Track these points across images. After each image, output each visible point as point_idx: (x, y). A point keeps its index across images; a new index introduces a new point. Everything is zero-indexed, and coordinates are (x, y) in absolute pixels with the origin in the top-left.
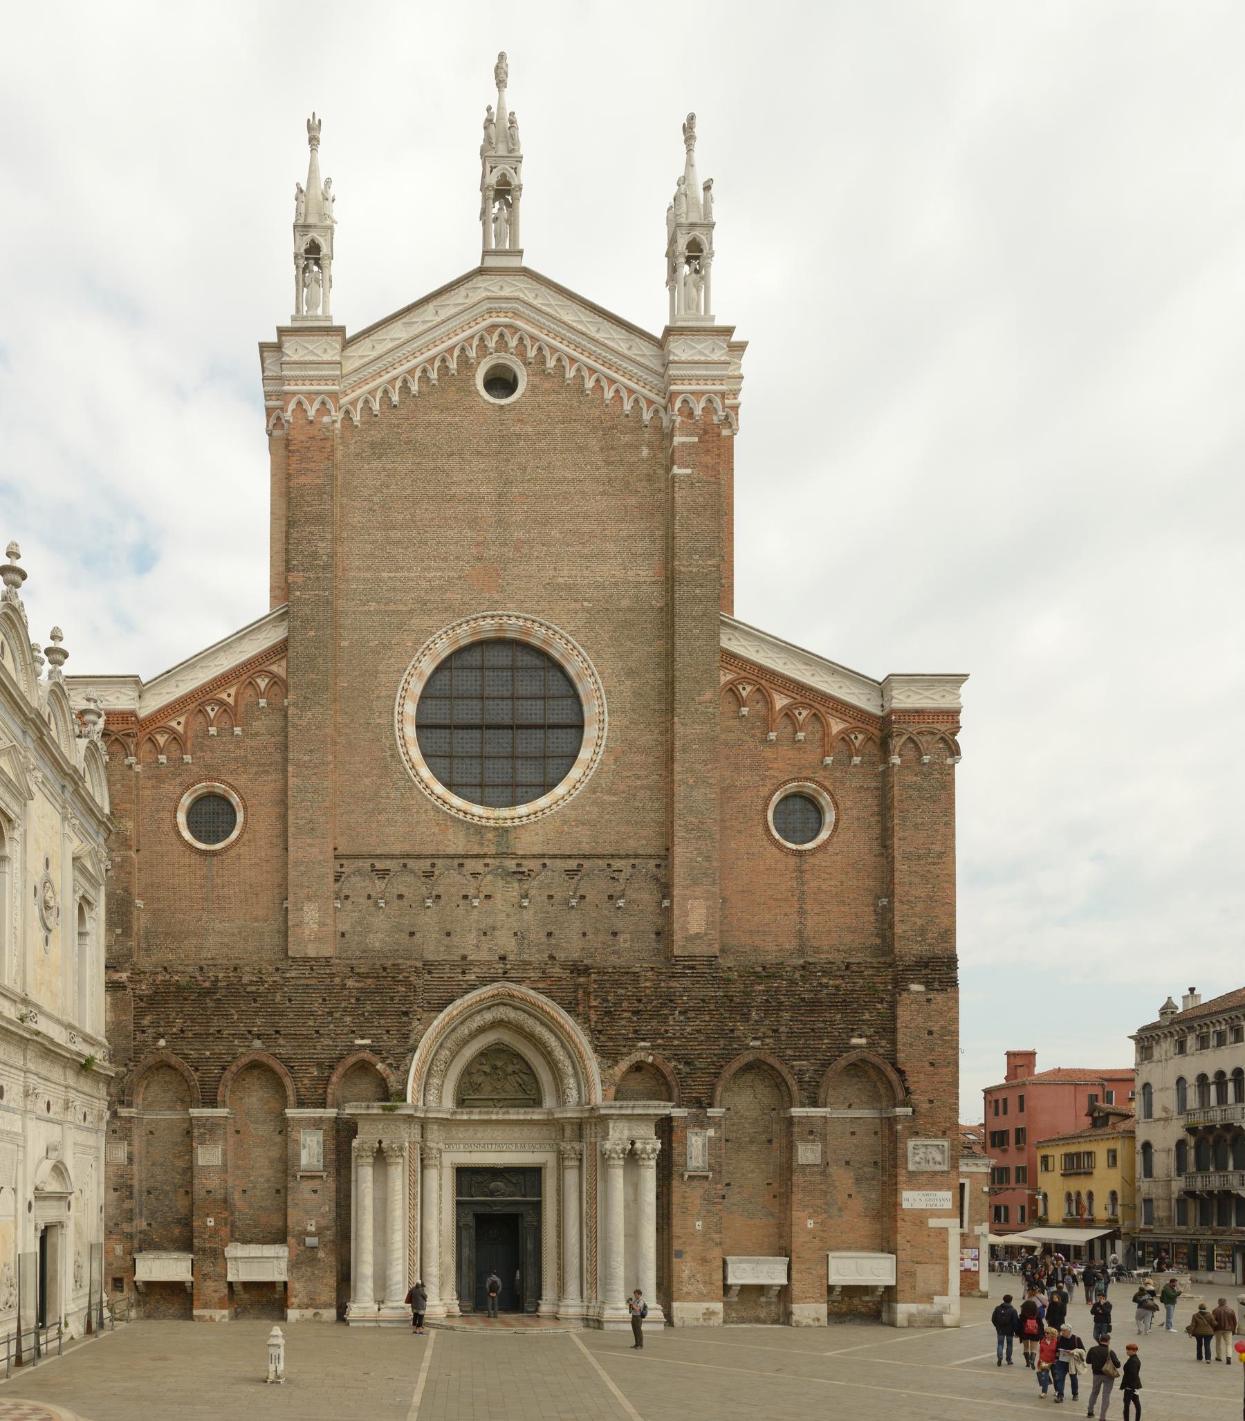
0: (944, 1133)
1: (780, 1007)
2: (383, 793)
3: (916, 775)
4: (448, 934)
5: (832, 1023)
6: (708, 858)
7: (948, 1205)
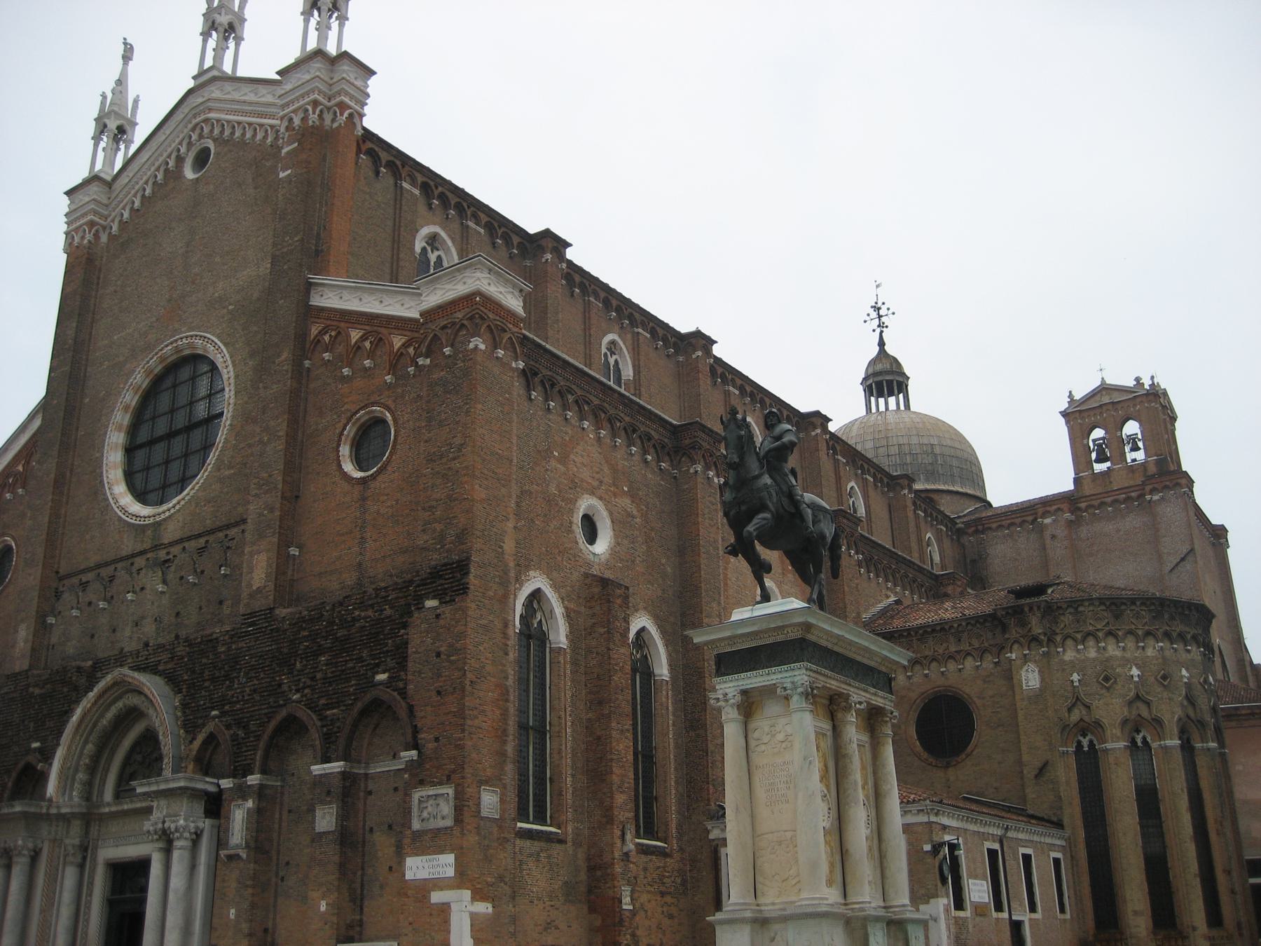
0: (449, 778)
3: (442, 370)
4: (114, 631)
5: (360, 659)
6: (272, 510)
7: (450, 872)
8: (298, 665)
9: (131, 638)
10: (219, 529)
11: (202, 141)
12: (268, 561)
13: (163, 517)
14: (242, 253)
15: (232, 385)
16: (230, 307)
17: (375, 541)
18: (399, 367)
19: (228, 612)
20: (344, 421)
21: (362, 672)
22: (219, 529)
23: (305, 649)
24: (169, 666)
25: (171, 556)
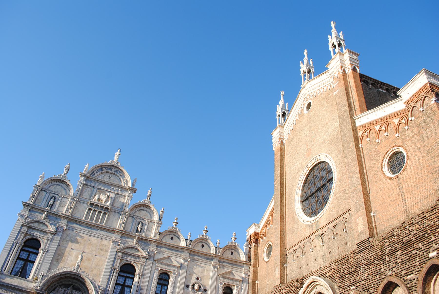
1: (396, 249)
2: (294, 227)
4: (308, 264)
5: (418, 249)
6: (360, 200)
8: (387, 259)
9: (314, 266)
10: (340, 216)
11: (308, 101)
12: (363, 220)
13: (318, 218)
14: (328, 124)
15: (334, 166)
16: (328, 142)
17: (410, 198)
18: (400, 129)
19: (350, 246)
20: (382, 158)
21: (421, 254)
22: (340, 216)
23: (389, 251)
24: (331, 273)
25: (324, 232)
